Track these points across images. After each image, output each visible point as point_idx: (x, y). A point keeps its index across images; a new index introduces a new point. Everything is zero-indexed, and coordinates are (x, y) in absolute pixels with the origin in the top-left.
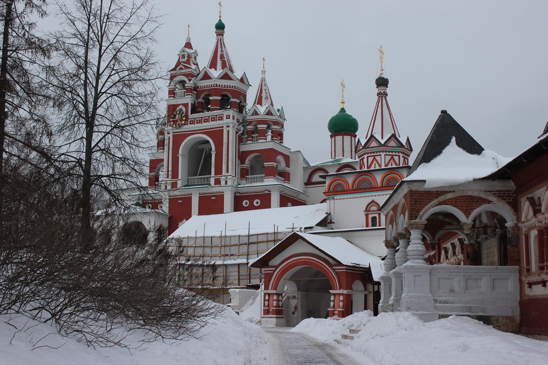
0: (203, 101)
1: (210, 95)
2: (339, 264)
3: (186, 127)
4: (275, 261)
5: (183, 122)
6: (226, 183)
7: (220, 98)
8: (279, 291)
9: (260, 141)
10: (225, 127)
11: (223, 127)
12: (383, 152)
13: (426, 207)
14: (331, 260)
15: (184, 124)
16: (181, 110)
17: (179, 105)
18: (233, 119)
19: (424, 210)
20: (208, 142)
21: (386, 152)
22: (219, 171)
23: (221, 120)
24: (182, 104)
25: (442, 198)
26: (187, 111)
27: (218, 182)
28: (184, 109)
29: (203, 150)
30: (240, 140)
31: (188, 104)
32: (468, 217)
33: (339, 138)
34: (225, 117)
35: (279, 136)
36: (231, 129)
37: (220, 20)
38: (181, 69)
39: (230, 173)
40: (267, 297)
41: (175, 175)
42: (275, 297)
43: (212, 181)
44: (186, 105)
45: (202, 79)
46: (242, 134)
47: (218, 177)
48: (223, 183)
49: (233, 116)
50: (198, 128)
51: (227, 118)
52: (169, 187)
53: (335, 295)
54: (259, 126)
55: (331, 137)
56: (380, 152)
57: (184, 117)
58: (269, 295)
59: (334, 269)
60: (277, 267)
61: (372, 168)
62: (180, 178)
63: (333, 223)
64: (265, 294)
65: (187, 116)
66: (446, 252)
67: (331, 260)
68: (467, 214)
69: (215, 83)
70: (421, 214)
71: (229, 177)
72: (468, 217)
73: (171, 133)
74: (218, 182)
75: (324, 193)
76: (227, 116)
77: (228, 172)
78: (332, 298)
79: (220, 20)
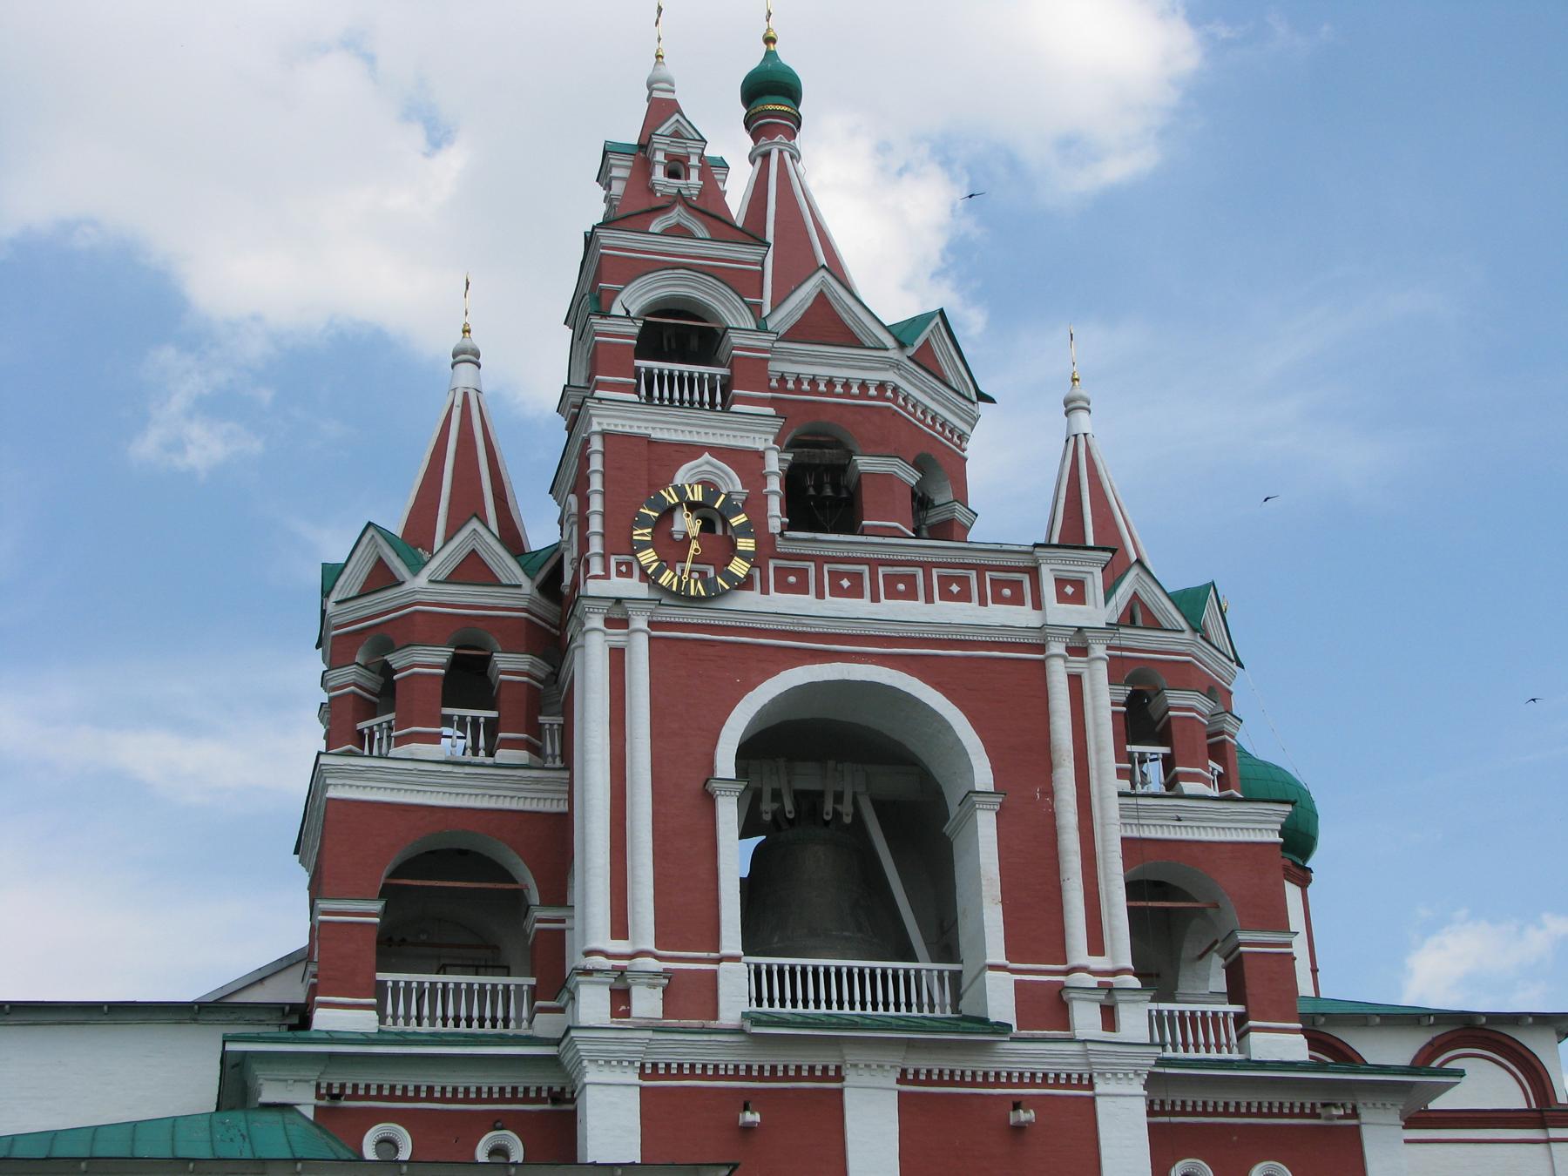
3: (749, 600)
6: (1109, 1018)
9: (1188, 787)
10: (1057, 648)
11: (1041, 648)
15: (746, 584)
16: (710, 489)
17: (691, 451)
23: (1017, 600)
24: (719, 452)
26: (754, 505)
27: (1046, 1009)
28: (732, 483)
31: (760, 456)
37: (770, 55)
38: (678, 231)
43: (999, 998)
44: (746, 462)
45: (797, 333)
47: (1041, 974)
48: (1085, 1018)
51: (1062, 598)
52: (648, 1002)
57: (744, 531)
65: (756, 527)
69: (890, 376)
71: (1118, 981)
73: (640, 622)
74: (1046, 1009)
76: (1060, 583)
79: (770, 55)
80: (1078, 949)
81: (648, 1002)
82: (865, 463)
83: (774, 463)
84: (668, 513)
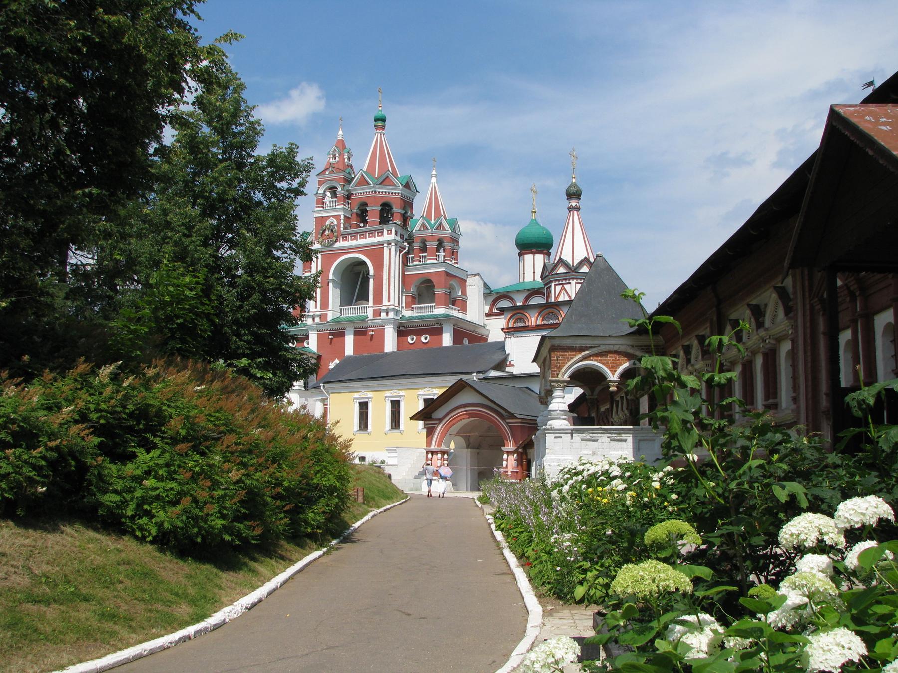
0: (359, 212)
1: (366, 205)
2: (512, 416)
3: (337, 245)
4: (439, 413)
5: (334, 239)
6: (387, 315)
7: (380, 208)
8: (443, 447)
12: (573, 279)
13: (569, 364)
14: (503, 412)
15: (336, 242)
17: (329, 217)
18: (396, 234)
19: (566, 366)
20: (363, 263)
21: (577, 279)
22: (378, 300)
25: (595, 351)
26: (338, 226)
28: (335, 223)
29: (359, 273)
30: (405, 261)
32: (613, 374)
33: (528, 258)
34: (385, 231)
35: (454, 254)
36: (393, 248)
39: (392, 303)
40: (430, 455)
41: (325, 305)
42: (439, 456)
43: (370, 313)
44: (337, 217)
46: (408, 253)
48: (383, 315)
49: (396, 232)
50: (353, 246)
52: (317, 320)
53: (508, 453)
54: (427, 243)
55: (520, 255)
56: (569, 279)
58: (432, 453)
59: (508, 423)
60: (440, 420)
61: (561, 299)
62: (330, 308)
63: (513, 366)
64: (427, 452)
66: (617, 406)
67: (503, 412)
68: (613, 373)
70: (563, 370)
72: (613, 374)
74: (377, 313)
75: (502, 329)
77: (389, 300)
78: (505, 456)
80: (385, 301)
81: (317, 320)
82: (368, 209)
83: (342, 217)
84: (324, 231)
